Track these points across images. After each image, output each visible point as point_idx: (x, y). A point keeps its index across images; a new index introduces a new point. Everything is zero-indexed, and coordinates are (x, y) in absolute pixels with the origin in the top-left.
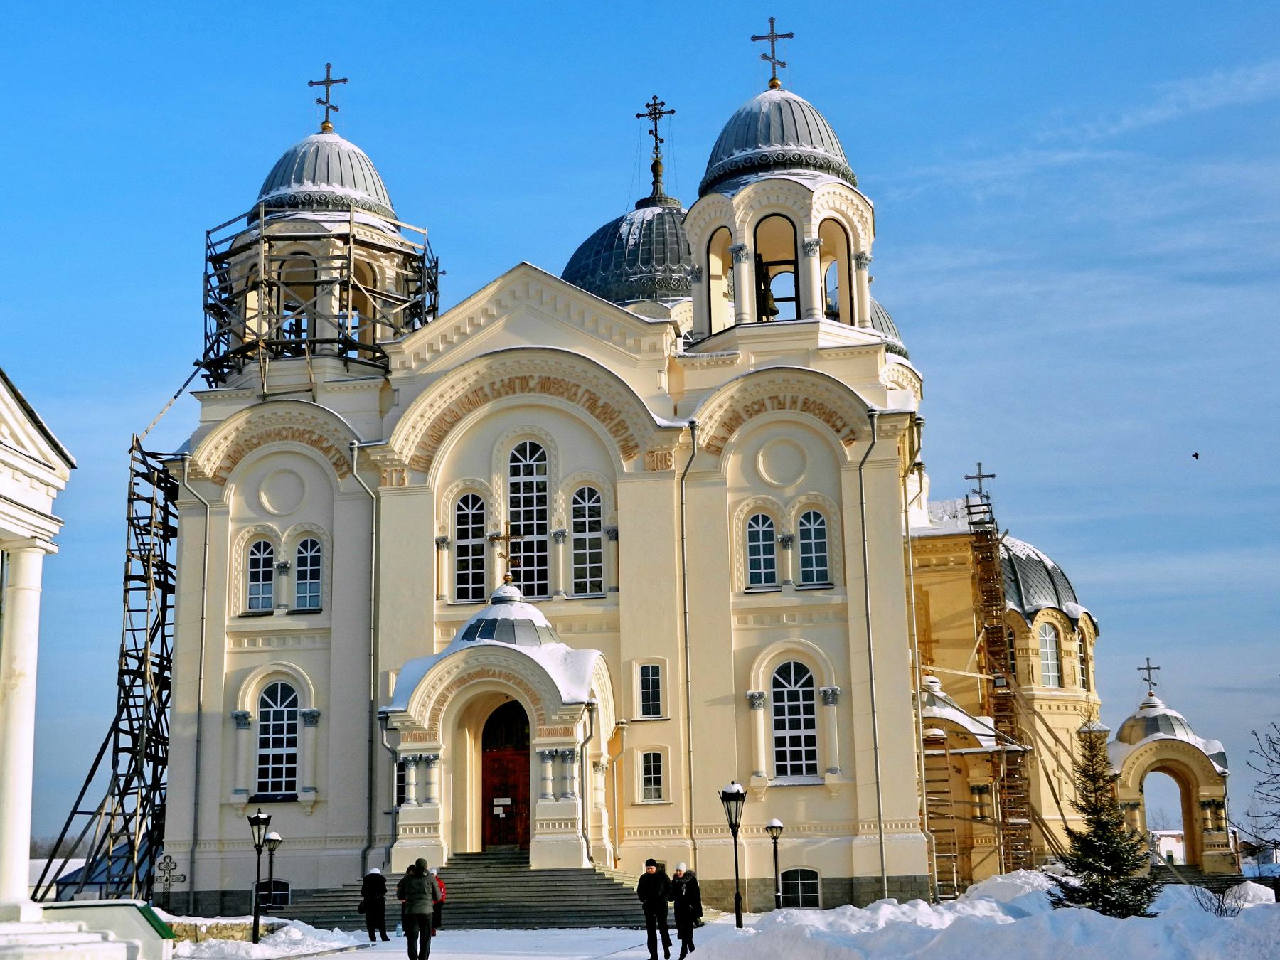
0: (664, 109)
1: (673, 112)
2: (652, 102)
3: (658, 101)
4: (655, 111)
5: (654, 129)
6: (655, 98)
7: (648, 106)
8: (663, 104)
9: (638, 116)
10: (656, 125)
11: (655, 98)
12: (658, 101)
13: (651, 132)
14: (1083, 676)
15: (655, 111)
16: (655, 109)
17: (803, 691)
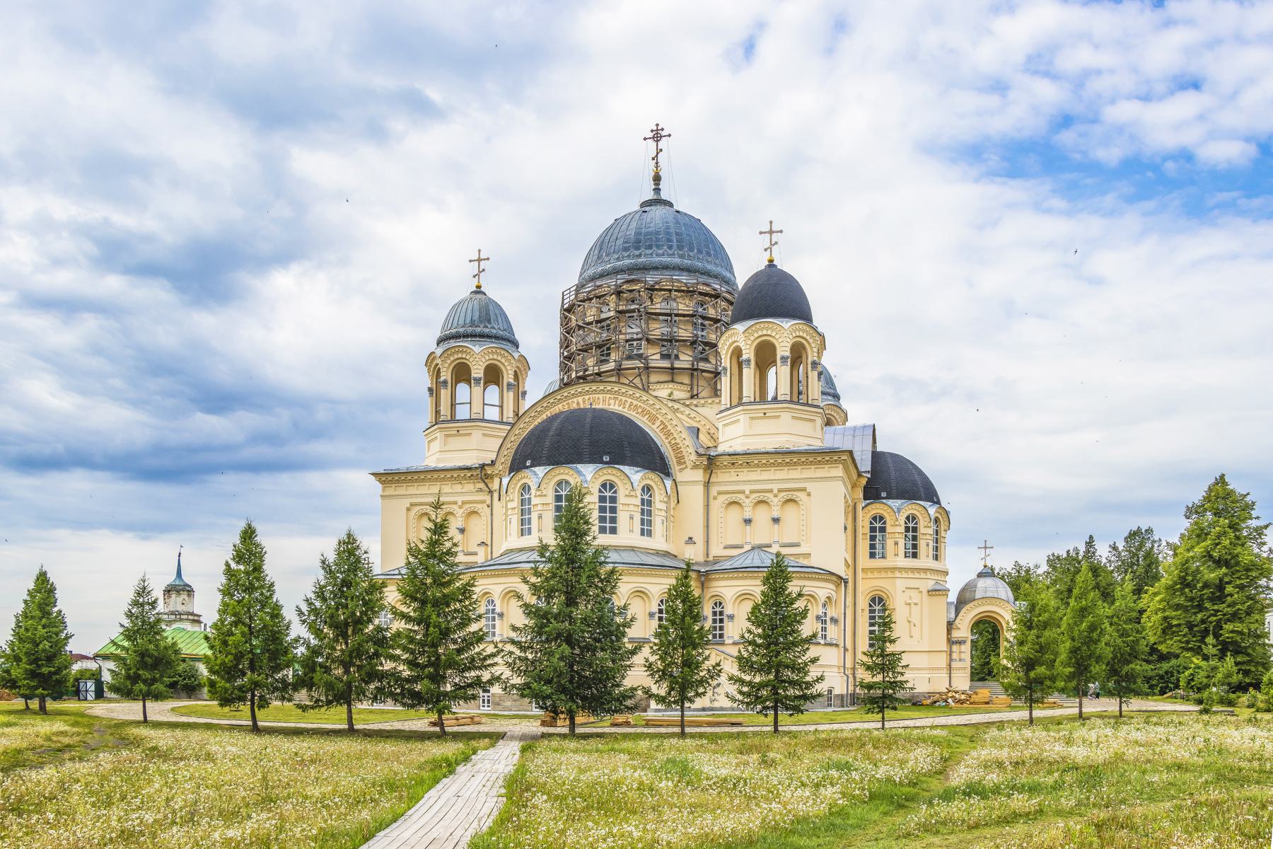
1: (669, 135)
6: (657, 125)
7: (652, 131)
8: (662, 129)
9: (645, 139)
11: (657, 125)
12: (659, 128)
15: (657, 136)
16: (657, 133)
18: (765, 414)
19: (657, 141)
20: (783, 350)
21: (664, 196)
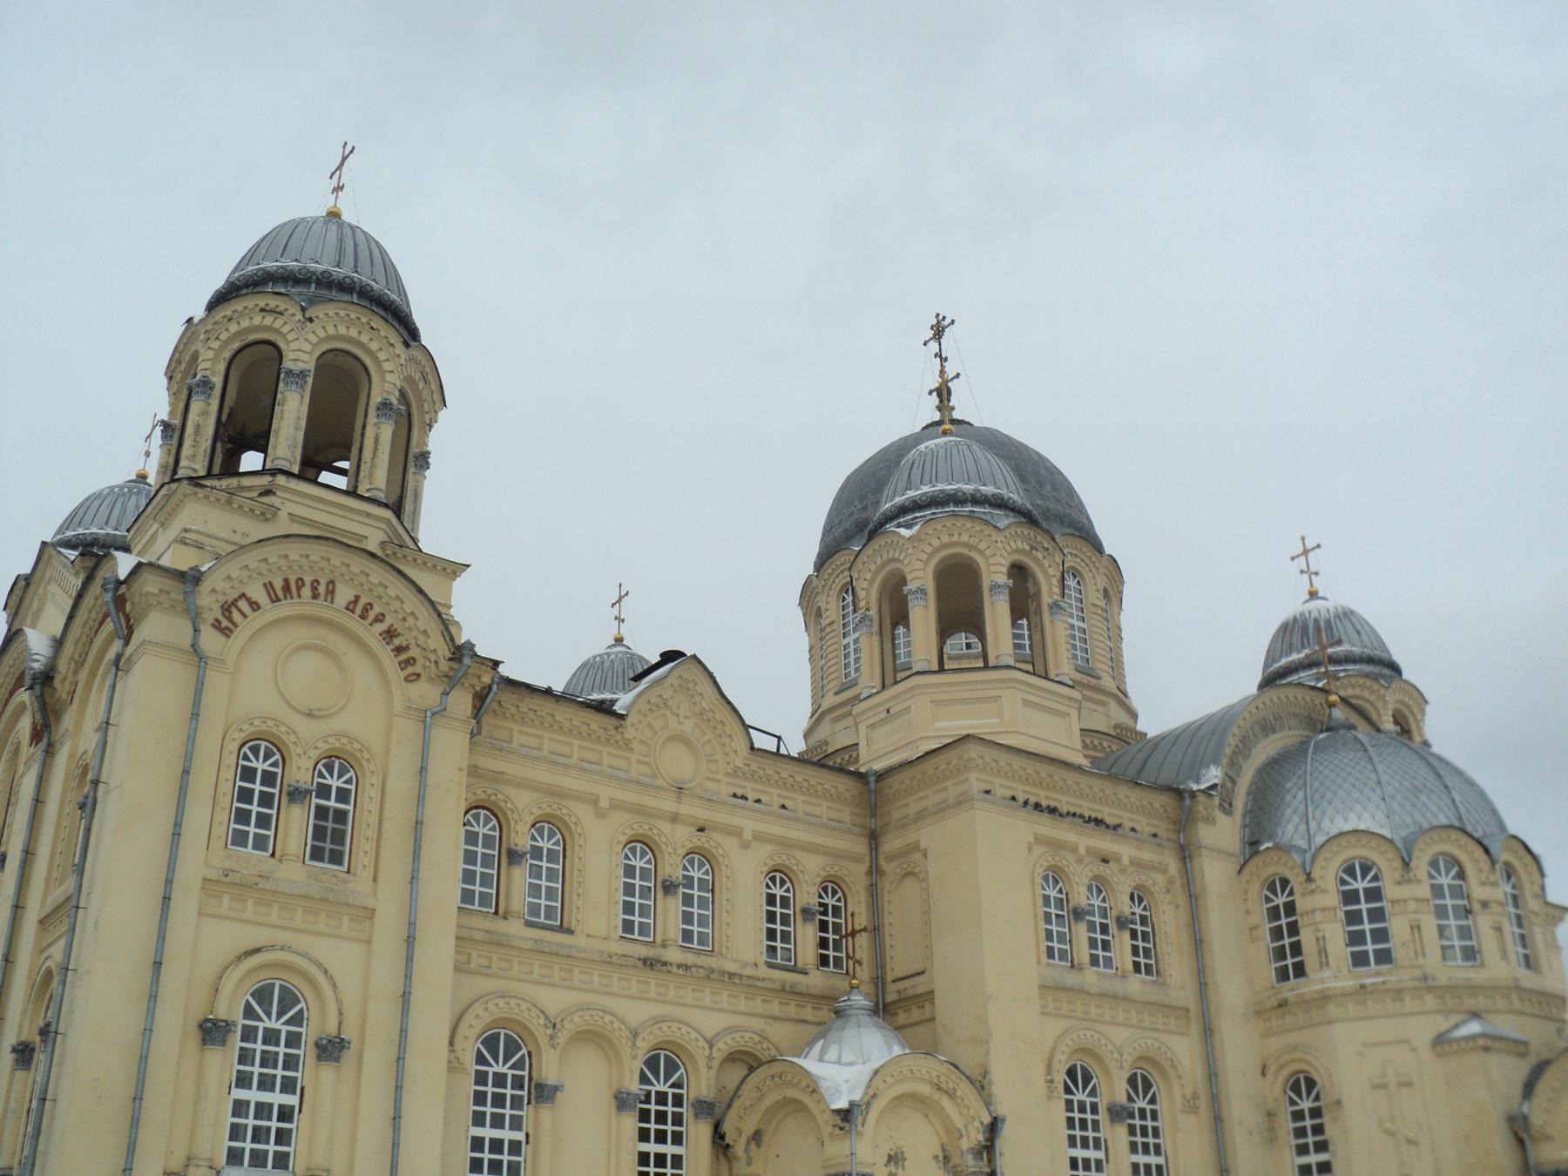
0: (946, 323)
1: (953, 322)
2: (935, 322)
3: (941, 318)
4: (939, 331)
6: (938, 315)
8: (944, 318)
10: (940, 344)
11: (938, 315)
12: (941, 318)
13: (936, 355)
15: (939, 331)
16: (938, 329)
17: (288, 1032)
18: (888, 711)
19: (940, 337)
20: (921, 578)
21: (956, 415)
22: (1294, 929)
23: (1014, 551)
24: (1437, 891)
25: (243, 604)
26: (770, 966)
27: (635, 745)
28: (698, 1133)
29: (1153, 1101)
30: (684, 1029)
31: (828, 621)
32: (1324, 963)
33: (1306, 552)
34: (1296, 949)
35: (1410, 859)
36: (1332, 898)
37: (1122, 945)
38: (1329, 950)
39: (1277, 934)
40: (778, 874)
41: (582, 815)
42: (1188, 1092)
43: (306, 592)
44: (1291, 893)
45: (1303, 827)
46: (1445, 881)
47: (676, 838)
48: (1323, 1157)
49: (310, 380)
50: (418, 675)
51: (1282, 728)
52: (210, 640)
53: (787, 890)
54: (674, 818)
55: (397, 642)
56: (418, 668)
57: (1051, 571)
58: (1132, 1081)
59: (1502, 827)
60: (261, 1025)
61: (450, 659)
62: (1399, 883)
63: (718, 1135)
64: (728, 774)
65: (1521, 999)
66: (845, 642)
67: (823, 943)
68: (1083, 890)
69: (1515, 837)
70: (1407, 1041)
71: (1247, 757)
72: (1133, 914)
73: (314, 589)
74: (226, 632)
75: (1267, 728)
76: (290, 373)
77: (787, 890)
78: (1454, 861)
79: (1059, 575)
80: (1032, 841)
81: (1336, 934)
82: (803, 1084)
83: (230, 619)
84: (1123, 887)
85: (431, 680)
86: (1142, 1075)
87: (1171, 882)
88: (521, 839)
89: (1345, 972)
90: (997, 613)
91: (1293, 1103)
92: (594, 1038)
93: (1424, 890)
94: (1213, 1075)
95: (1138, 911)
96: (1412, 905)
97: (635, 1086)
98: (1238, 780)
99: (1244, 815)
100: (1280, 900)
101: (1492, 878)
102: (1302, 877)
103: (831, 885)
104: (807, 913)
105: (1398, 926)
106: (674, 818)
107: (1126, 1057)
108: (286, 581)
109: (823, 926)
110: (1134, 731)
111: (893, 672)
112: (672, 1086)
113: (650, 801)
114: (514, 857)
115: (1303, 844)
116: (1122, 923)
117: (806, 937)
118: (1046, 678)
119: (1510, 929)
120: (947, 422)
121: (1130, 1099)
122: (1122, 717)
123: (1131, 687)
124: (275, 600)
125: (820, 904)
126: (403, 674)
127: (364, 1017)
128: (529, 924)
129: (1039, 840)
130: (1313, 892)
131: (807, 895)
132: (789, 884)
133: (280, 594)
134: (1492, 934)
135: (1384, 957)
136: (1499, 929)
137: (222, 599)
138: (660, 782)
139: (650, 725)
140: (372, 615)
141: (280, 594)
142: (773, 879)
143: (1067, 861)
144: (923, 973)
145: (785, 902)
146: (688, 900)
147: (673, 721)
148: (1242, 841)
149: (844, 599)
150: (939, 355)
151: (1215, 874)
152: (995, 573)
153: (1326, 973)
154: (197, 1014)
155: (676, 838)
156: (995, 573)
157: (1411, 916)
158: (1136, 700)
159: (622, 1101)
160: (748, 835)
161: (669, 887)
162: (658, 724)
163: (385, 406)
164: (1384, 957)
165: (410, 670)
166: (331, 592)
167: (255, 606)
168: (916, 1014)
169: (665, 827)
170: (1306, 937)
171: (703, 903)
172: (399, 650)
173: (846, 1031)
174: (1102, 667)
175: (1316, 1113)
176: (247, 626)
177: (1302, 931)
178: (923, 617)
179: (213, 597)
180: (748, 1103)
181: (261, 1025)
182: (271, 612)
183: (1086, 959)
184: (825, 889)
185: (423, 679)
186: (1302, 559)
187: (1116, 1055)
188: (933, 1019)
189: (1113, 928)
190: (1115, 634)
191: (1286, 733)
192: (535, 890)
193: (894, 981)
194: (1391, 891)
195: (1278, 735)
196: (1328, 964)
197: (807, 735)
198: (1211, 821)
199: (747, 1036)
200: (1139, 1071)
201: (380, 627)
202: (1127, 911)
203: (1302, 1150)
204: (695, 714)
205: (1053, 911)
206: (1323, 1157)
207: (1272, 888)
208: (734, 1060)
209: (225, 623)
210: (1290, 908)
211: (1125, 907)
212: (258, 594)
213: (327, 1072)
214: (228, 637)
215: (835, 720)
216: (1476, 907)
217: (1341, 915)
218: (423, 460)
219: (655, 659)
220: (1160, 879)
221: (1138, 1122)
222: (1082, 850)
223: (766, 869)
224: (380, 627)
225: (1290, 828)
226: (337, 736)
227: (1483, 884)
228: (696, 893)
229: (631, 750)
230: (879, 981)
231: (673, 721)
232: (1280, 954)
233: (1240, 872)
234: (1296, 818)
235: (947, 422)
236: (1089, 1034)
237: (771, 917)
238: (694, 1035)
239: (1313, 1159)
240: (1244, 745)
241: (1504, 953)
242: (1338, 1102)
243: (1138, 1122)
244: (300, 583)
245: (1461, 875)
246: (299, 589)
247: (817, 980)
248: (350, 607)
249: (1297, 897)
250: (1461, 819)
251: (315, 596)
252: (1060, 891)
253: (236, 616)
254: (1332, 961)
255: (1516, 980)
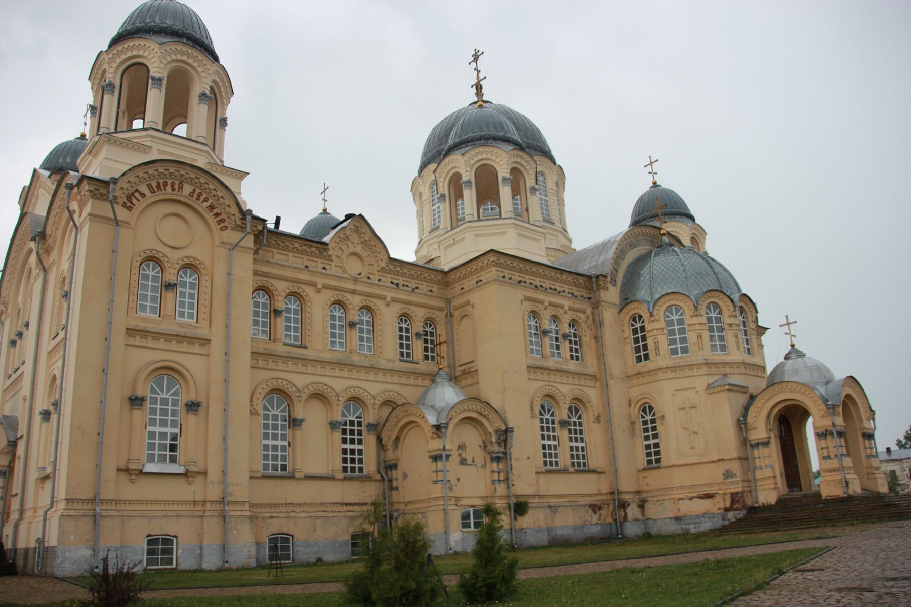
3: (477, 51)
4: (476, 57)
5: (475, 67)
6: (476, 49)
8: (479, 51)
11: (476, 49)
12: (477, 51)
13: (475, 69)
14: (747, 344)
15: (476, 57)
18: (454, 240)
19: (477, 60)
20: (467, 175)
21: (485, 98)
22: (644, 338)
23: (513, 163)
24: (710, 320)
25: (137, 195)
26: (401, 361)
27: (333, 258)
28: (370, 440)
29: (580, 418)
30: (361, 391)
31: (425, 198)
32: (658, 353)
33: (651, 164)
34: (645, 347)
35: (698, 305)
36: (662, 324)
37: (565, 346)
38: (660, 348)
39: (636, 341)
40: (405, 317)
41: (309, 291)
42: (596, 414)
43: (169, 188)
44: (643, 322)
45: (649, 291)
46: (713, 315)
47: (355, 301)
48: (656, 441)
49: (165, 82)
50: (226, 227)
51: (639, 245)
52: (122, 213)
53: (408, 325)
54: (354, 292)
55: (215, 211)
56: (226, 224)
57: (531, 172)
58: (570, 409)
59: (739, 290)
60: (159, 397)
61: (242, 219)
62: (692, 316)
63: (379, 439)
64: (379, 271)
65: (745, 368)
66: (433, 208)
67: (426, 349)
68: (547, 322)
69: (744, 295)
70: (694, 388)
71: (623, 259)
72: (570, 332)
73: (172, 186)
74: (129, 209)
75: (633, 246)
76: (153, 79)
77: (408, 325)
78: (716, 306)
79: (534, 174)
80: (523, 299)
81: (663, 340)
82: (418, 415)
83: (131, 202)
84: (566, 319)
85: (233, 229)
86: (575, 406)
87: (587, 318)
88: (281, 304)
89: (667, 357)
90: (505, 192)
91: (643, 417)
92: (319, 396)
93: (704, 320)
94: (607, 404)
95: (573, 331)
96: (698, 327)
97: (339, 418)
98: (619, 270)
99: (622, 287)
100: (638, 325)
101: (734, 314)
102: (648, 314)
103: (429, 321)
104: (418, 335)
105: (691, 337)
106: (354, 292)
107: (567, 398)
108: (158, 183)
109: (426, 341)
110: (570, 248)
111: (456, 221)
112: (357, 417)
113: (343, 285)
114: (277, 312)
115: (649, 300)
116: (565, 337)
117: (418, 347)
118: (529, 223)
119: (742, 336)
120: (481, 101)
121: (569, 417)
122: (563, 241)
123: (569, 228)
124: (153, 191)
125: (424, 331)
126: (219, 227)
127: (208, 391)
128: (285, 345)
129: (527, 299)
130: (653, 321)
131: (418, 327)
132: (409, 322)
133: (155, 189)
134: (734, 339)
135: (685, 350)
136: (737, 337)
137: (126, 192)
138: (346, 276)
139: (340, 248)
140: (202, 198)
141: (155, 189)
142: (401, 320)
143: (539, 308)
144: (473, 362)
145: (407, 330)
146: (361, 331)
147: (351, 246)
148: (621, 298)
149: (432, 188)
150: (476, 69)
151: (608, 315)
152: (503, 172)
153: (659, 357)
154: (128, 393)
155: (355, 301)
156: (503, 172)
157: (698, 332)
158: (571, 233)
159: (333, 425)
160: (389, 299)
161: (352, 325)
162: (344, 248)
163: (203, 95)
164: (685, 350)
165: (222, 225)
166: (181, 188)
167: (143, 195)
168: (470, 381)
169: (349, 296)
170: (650, 342)
171: (368, 332)
172: (217, 215)
173: (437, 390)
174: (555, 218)
175: (653, 421)
176: (140, 205)
177: (648, 339)
178: (470, 195)
179: (122, 192)
180: (392, 424)
181: (159, 397)
182: (151, 198)
183: (549, 354)
184: (426, 324)
185: (229, 228)
186: (650, 166)
187: (563, 398)
188: (477, 383)
189: (561, 339)
190: (561, 202)
191: (641, 248)
192: (288, 328)
193: (459, 366)
194: (688, 320)
195: (638, 249)
196: (659, 354)
197: (416, 253)
198: (606, 289)
199: (391, 393)
200: (573, 405)
201: (206, 205)
202: (567, 331)
203: (647, 438)
204: (362, 243)
205: (533, 332)
206: (656, 441)
207: (634, 320)
208: (385, 404)
209: (129, 204)
210: (643, 329)
211: (566, 329)
212: (144, 189)
213: (192, 418)
214: (131, 211)
215: (429, 246)
216: (727, 327)
217: (665, 331)
218: (224, 122)
219: (342, 218)
220: (582, 316)
221: (573, 428)
222: (546, 303)
223: (398, 315)
224: (206, 205)
225: (643, 292)
226: (188, 258)
227: (730, 316)
228: (365, 327)
229: (332, 260)
230: (452, 366)
231: (351, 246)
232: (637, 350)
233: (619, 312)
234: (646, 287)
235: (481, 101)
236: (550, 388)
237: (401, 338)
238: (366, 394)
239: (652, 442)
240: (622, 254)
241: (738, 348)
242: (663, 416)
243: (573, 428)
244: (165, 184)
245: (720, 312)
246: (165, 186)
247: (424, 366)
248: (192, 194)
249: (646, 324)
250: (721, 287)
251: (173, 190)
252: (536, 322)
253: (134, 201)
254: (661, 353)
255: (744, 360)
